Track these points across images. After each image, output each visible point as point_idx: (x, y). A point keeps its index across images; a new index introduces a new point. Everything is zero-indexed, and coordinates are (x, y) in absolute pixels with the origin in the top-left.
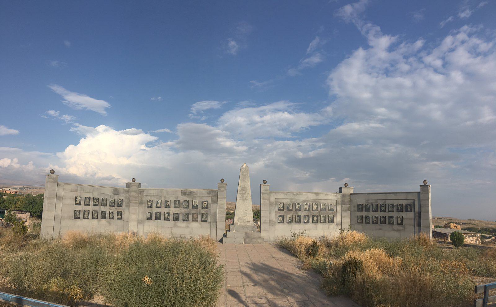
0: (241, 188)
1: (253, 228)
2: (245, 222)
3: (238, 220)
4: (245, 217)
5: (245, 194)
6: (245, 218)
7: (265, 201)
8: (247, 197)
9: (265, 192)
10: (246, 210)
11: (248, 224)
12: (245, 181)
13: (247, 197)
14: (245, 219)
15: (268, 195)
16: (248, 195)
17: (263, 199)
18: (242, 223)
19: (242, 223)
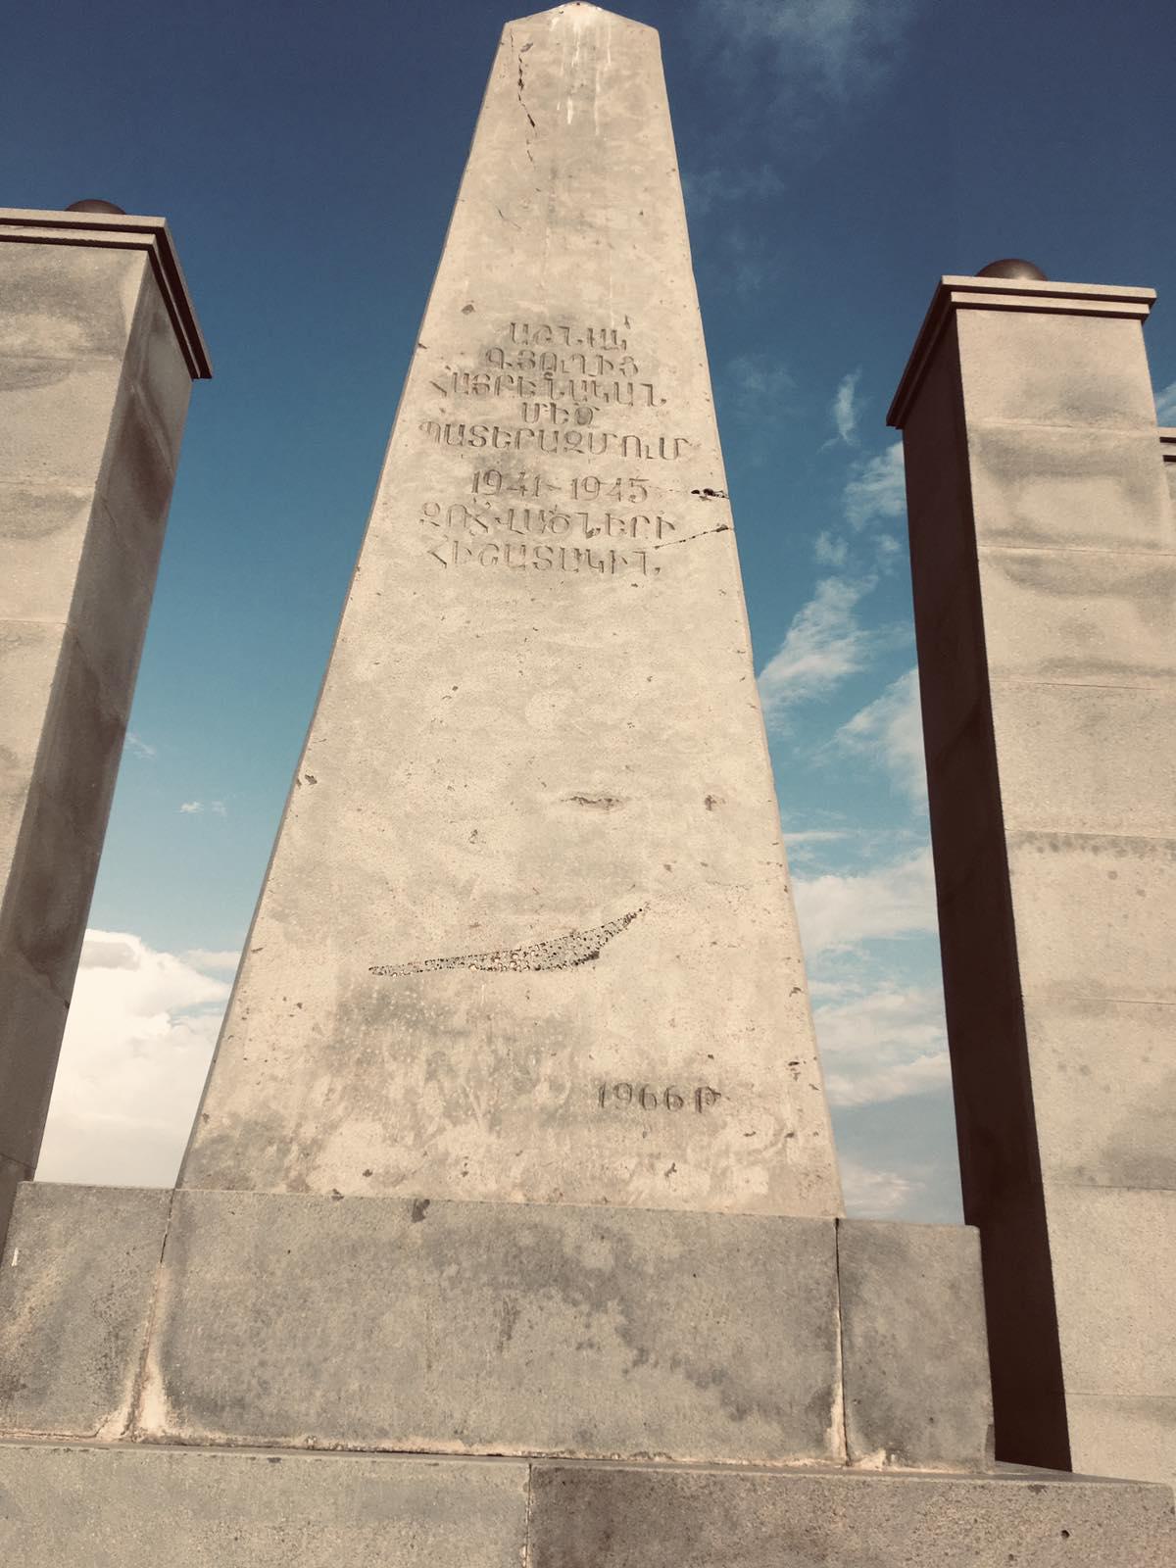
0: (488, 327)
1: (845, 1285)
2: (557, 1118)
3: (335, 1054)
4: (551, 958)
5: (568, 443)
6: (558, 990)
7: (1081, 631)
8: (624, 508)
9: (1056, 434)
10: (597, 783)
11: (647, 1188)
12: (582, 223)
13: (624, 508)
14: (560, 1033)
15: (1138, 493)
16: (656, 472)
17: (1029, 575)
18: (468, 1140)
19: (468, 1140)
